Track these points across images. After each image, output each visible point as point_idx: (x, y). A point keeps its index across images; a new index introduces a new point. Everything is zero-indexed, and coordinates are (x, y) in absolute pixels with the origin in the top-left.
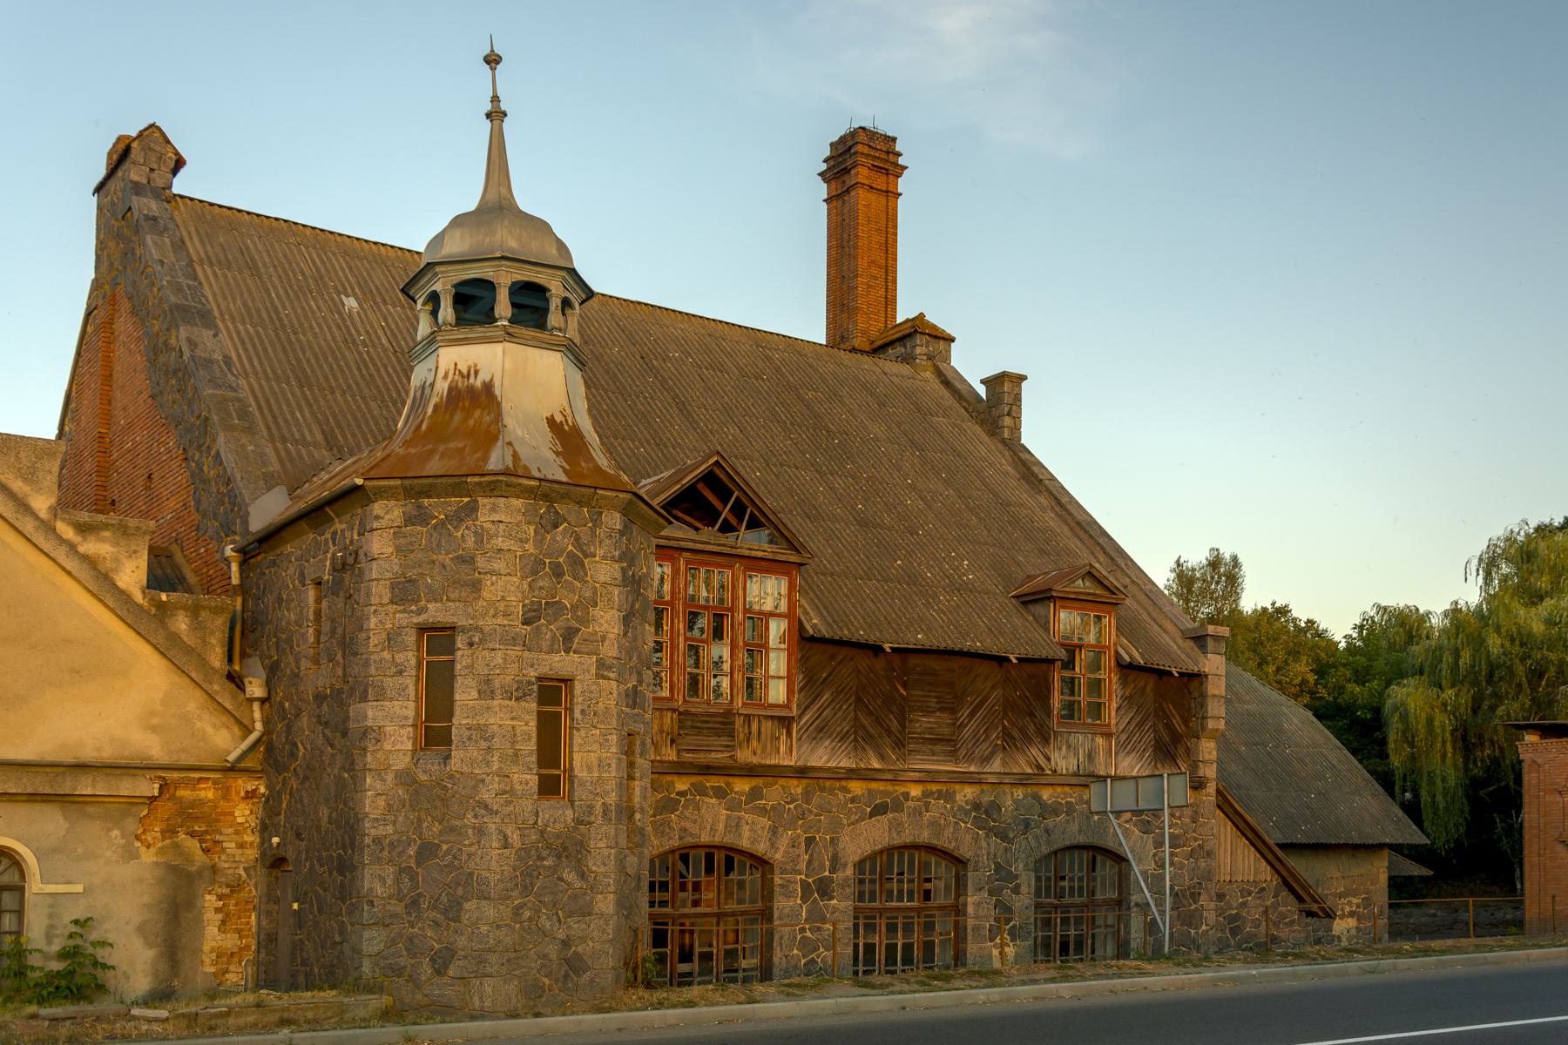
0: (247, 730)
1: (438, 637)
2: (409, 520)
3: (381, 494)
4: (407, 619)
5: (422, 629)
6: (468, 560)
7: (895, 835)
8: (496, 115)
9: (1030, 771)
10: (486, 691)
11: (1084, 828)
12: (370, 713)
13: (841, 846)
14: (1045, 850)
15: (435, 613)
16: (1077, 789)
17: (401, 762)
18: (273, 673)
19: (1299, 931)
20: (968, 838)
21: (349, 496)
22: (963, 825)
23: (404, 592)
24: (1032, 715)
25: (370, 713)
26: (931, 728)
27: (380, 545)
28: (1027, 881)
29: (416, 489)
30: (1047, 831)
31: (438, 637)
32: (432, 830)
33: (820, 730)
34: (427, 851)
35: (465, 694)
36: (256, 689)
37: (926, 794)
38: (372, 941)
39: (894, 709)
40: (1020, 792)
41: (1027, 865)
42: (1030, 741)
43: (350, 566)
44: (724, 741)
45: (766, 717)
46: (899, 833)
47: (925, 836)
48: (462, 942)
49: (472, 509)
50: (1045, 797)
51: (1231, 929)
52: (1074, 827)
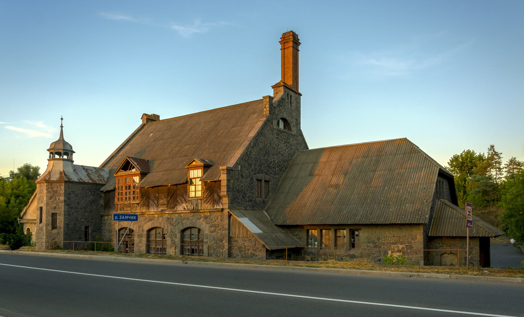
7: (153, 225)
8: (62, 127)
9: (182, 210)
11: (191, 223)
13: (144, 227)
14: (182, 228)
16: (189, 213)
19: (263, 253)
20: (166, 226)
22: (165, 223)
24: (183, 197)
26: (163, 202)
30: (182, 224)
33: (144, 205)
37: (158, 216)
39: (156, 199)
40: (177, 215)
41: (178, 232)
42: (183, 203)
44: (130, 208)
45: (136, 203)
46: (153, 225)
47: (158, 225)
50: (182, 216)
51: (239, 251)
52: (188, 223)
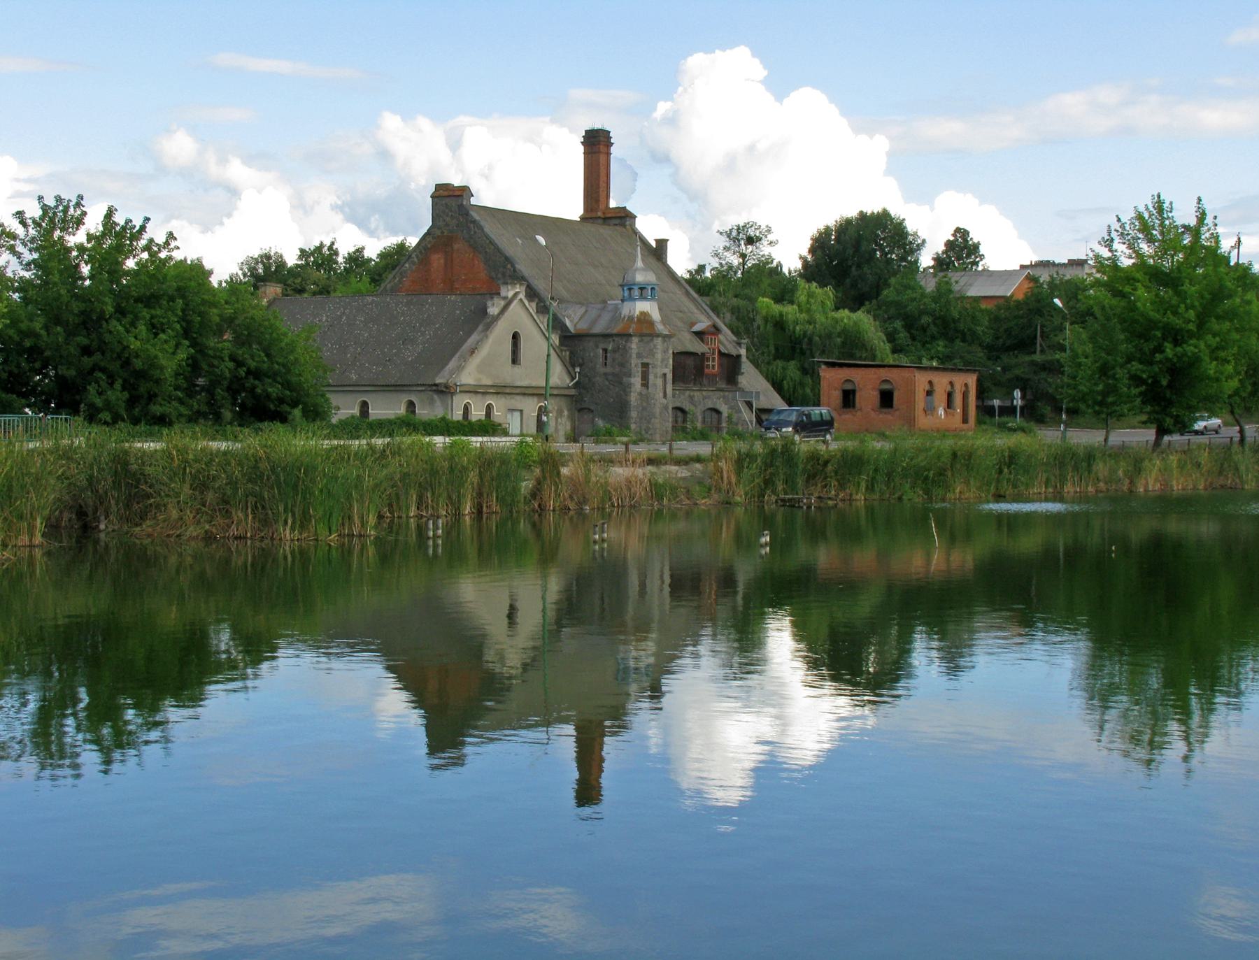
0: (573, 379)
1: (645, 365)
2: (639, 341)
3: (635, 336)
4: (640, 361)
5: (642, 364)
6: (652, 350)
10: (656, 377)
12: (633, 380)
15: (645, 360)
17: (638, 390)
18: (581, 366)
21: (630, 335)
23: (639, 356)
25: (633, 380)
27: (634, 346)
28: (700, 418)
29: (642, 335)
31: (645, 365)
32: (645, 404)
34: (644, 409)
35: (651, 377)
36: (578, 370)
38: (633, 426)
43: (625, 351)
48: (651, 427)
49: (652, 340)
